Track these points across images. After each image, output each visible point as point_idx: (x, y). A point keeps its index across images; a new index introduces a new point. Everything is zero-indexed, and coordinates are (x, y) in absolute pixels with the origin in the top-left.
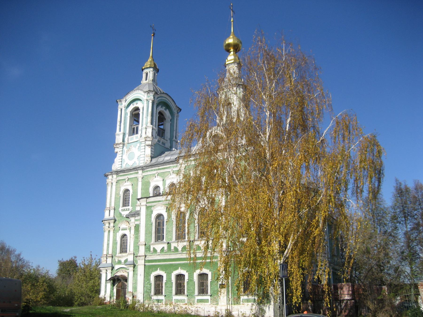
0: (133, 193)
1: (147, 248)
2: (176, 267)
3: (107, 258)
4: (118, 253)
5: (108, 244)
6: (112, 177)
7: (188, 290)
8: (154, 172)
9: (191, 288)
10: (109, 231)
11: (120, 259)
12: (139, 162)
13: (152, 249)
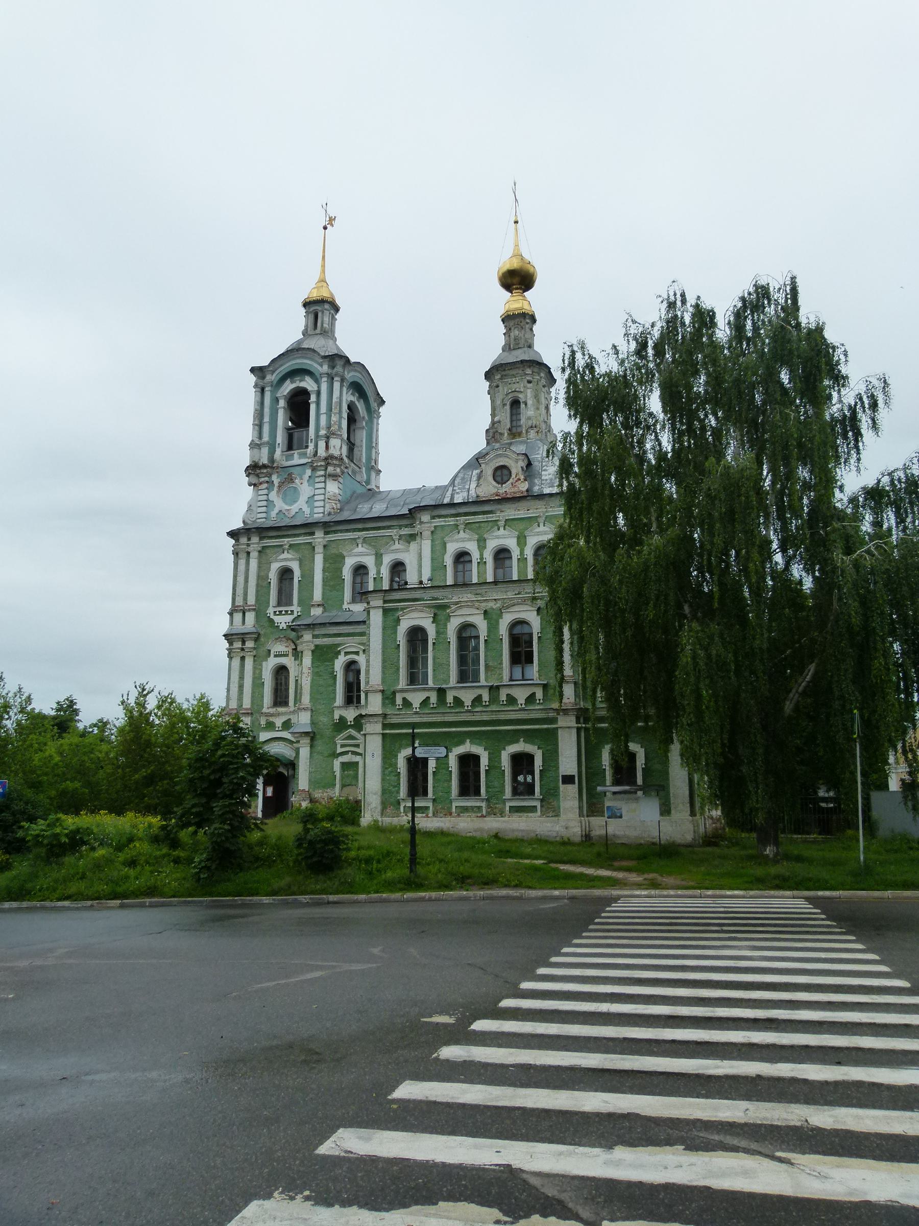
0: (302, 576)
1: (387, 698)
2: (459, 739)
4: (265, 705)
5: (241, 687)
6: (249, 539)
7: (487, 787)
9: (496, 784)
10: (243, 658)
11: (271, 719)
12: (312, 510)
13: (399, 701)
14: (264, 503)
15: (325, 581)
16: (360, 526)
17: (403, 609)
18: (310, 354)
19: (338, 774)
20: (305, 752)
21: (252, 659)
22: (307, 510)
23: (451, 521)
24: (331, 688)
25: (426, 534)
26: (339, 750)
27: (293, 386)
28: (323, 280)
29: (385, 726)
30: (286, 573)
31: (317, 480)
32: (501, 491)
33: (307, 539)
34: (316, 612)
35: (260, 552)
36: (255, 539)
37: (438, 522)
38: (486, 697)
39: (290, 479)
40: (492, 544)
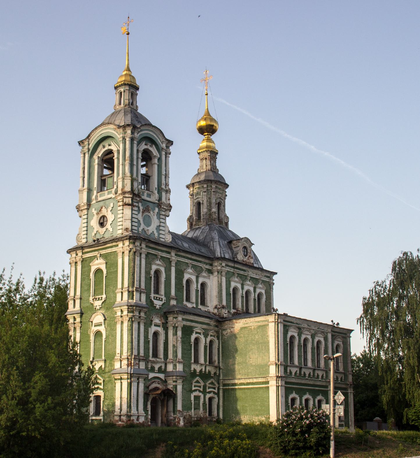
0: (166, 278)
3: (139, 361)
6: (141, 245)
10: (139, 323)
11: (153, 365)
13: (288, 371)
14: (136, 220)
16: (190, 256)
18: (158, 133)
19: (193, 402)
20: (180, 388)
21: (143, 324)
22: (156, 235)
24: (190, 352)
25: (224, 273)
26: (193, 388)
27: (146, 147)
30: (157, 273)
31: (162, 217)
32: (245, 260)
33: (167, 256)
34: (173, 302)
35: (146, 255)
36: (143, 246)
37: (228, 269)
38: (312, 374)
40: (246, 288)
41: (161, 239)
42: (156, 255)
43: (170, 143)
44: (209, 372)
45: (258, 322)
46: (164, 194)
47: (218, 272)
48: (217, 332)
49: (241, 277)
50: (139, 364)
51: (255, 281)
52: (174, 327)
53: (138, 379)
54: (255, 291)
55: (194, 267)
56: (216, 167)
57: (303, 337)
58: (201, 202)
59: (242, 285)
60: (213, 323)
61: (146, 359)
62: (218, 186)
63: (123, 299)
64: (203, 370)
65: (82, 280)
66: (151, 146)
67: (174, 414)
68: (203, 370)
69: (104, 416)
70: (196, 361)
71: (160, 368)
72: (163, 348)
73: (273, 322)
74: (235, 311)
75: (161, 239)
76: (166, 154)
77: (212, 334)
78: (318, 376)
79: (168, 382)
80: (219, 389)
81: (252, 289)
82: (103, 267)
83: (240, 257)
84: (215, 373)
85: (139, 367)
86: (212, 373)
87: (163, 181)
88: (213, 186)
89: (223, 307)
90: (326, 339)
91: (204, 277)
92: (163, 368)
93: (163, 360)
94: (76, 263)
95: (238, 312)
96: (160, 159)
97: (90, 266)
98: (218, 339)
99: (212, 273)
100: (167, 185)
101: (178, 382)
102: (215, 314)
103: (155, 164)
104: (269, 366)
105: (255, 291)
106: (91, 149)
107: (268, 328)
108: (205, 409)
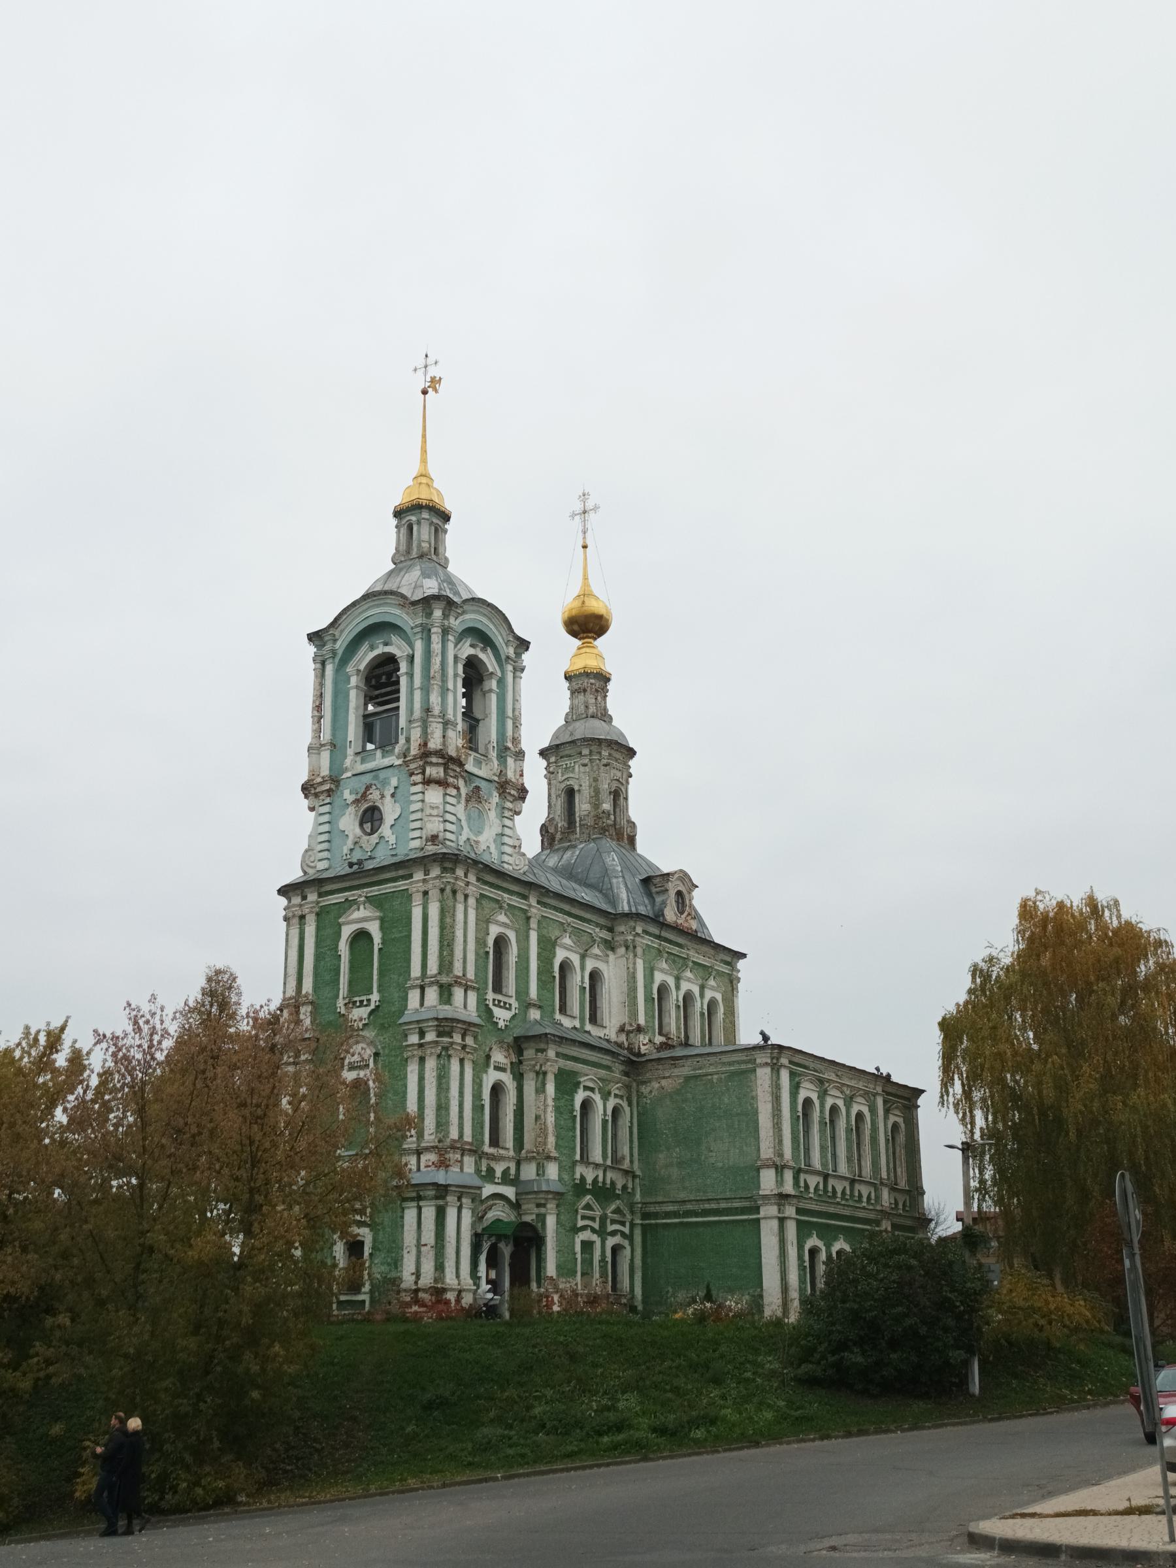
0: (519, 956)
3: (462, 1155)
6: (466, 875)
8: (570, 920)
11: (493, 1164)
13: (802, 1184)
15: (540, 973)
16: (567, 907)
17: (800, 1075)
19: (579, 1256)
20: (551, 1221)
23: (656, 944)
26: (580, 1223)
27: (472, 651)
28: (423, 476)
29: (799, 1211)
31: (507, 814)
32: (679, 922)
35: (477, 900)
36: (472, 878)
37: (647, 940)
39: (475, 796)
40: (685, 986)
41: (505, 866)
42: (497, 901)
43: (523, 645)
44: (613, 1183)
45: (730, 1064)
46: (510, 761)
47: (627, 948)
48: (628, 1087)
49: (674, 962)
50: (461, 1162)
51: (705, 971)
52: (537, 1073)
53: (459, 1199)
54: (702, 995)
55: (576, 933)
56: (605, 709)
57: (829, 1102)
58: (576, 788)
59: (678, 979)
60: (618, 1068)
61: (475, 1151)
62: (613, 752)
63: (426, 1003)
64: (601, 1179)
65: (318, 957)
66: (484, 650)
67: (539, 1286)
68: (601, 1179)
69: (371, 1292)
70: (585, 1159)
71: (506, 1172)
72: (512, 1124)
73: (767, 1064)
74: (663, 1039)
75: (505, 866)
76: (515, 669)
77: (617, 1092)
78: (860, 1195)
79: (524, 1207)
80: (632, 1226)
81: (696, 990)
82: (374, 928)
83: (670, 915)
84: (624, 1187)
85: (462, 1169)
86: (619, 1186)
87: (509, 733)
88: (603, 753)
89: (639, 1029)
90: (873, 1110)
91: (596, 957)
92: (513, 1171)
93: (512, 1153)
94: (302, 917)
95: (670, 1042)
96: (501, 682)
97: (340, 925)
98: (630, 1105)
99: (613, 949)
100: (516, 740)
101: (549, 1206)
102: (620, 1045)
103: (491, 691)
104: (758, 1170)
105: (702, 995)
106: (340, 652)
107: (753, 1077)
108: (603, 1274)
